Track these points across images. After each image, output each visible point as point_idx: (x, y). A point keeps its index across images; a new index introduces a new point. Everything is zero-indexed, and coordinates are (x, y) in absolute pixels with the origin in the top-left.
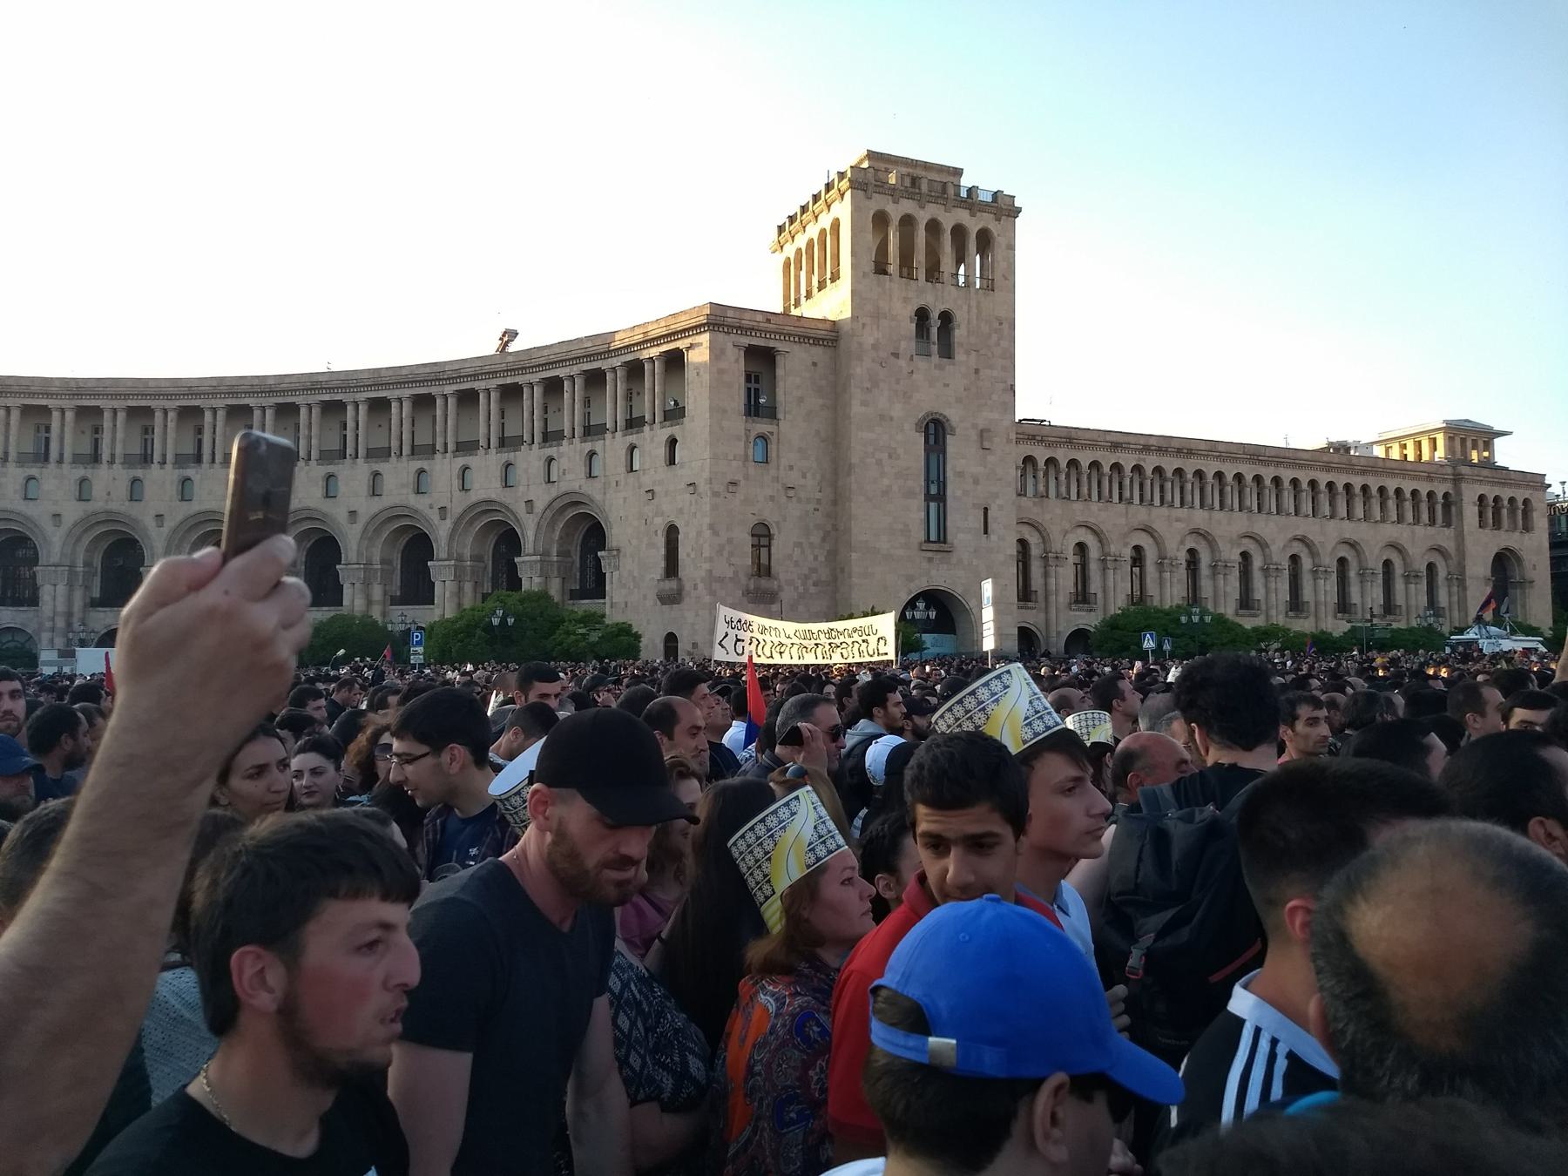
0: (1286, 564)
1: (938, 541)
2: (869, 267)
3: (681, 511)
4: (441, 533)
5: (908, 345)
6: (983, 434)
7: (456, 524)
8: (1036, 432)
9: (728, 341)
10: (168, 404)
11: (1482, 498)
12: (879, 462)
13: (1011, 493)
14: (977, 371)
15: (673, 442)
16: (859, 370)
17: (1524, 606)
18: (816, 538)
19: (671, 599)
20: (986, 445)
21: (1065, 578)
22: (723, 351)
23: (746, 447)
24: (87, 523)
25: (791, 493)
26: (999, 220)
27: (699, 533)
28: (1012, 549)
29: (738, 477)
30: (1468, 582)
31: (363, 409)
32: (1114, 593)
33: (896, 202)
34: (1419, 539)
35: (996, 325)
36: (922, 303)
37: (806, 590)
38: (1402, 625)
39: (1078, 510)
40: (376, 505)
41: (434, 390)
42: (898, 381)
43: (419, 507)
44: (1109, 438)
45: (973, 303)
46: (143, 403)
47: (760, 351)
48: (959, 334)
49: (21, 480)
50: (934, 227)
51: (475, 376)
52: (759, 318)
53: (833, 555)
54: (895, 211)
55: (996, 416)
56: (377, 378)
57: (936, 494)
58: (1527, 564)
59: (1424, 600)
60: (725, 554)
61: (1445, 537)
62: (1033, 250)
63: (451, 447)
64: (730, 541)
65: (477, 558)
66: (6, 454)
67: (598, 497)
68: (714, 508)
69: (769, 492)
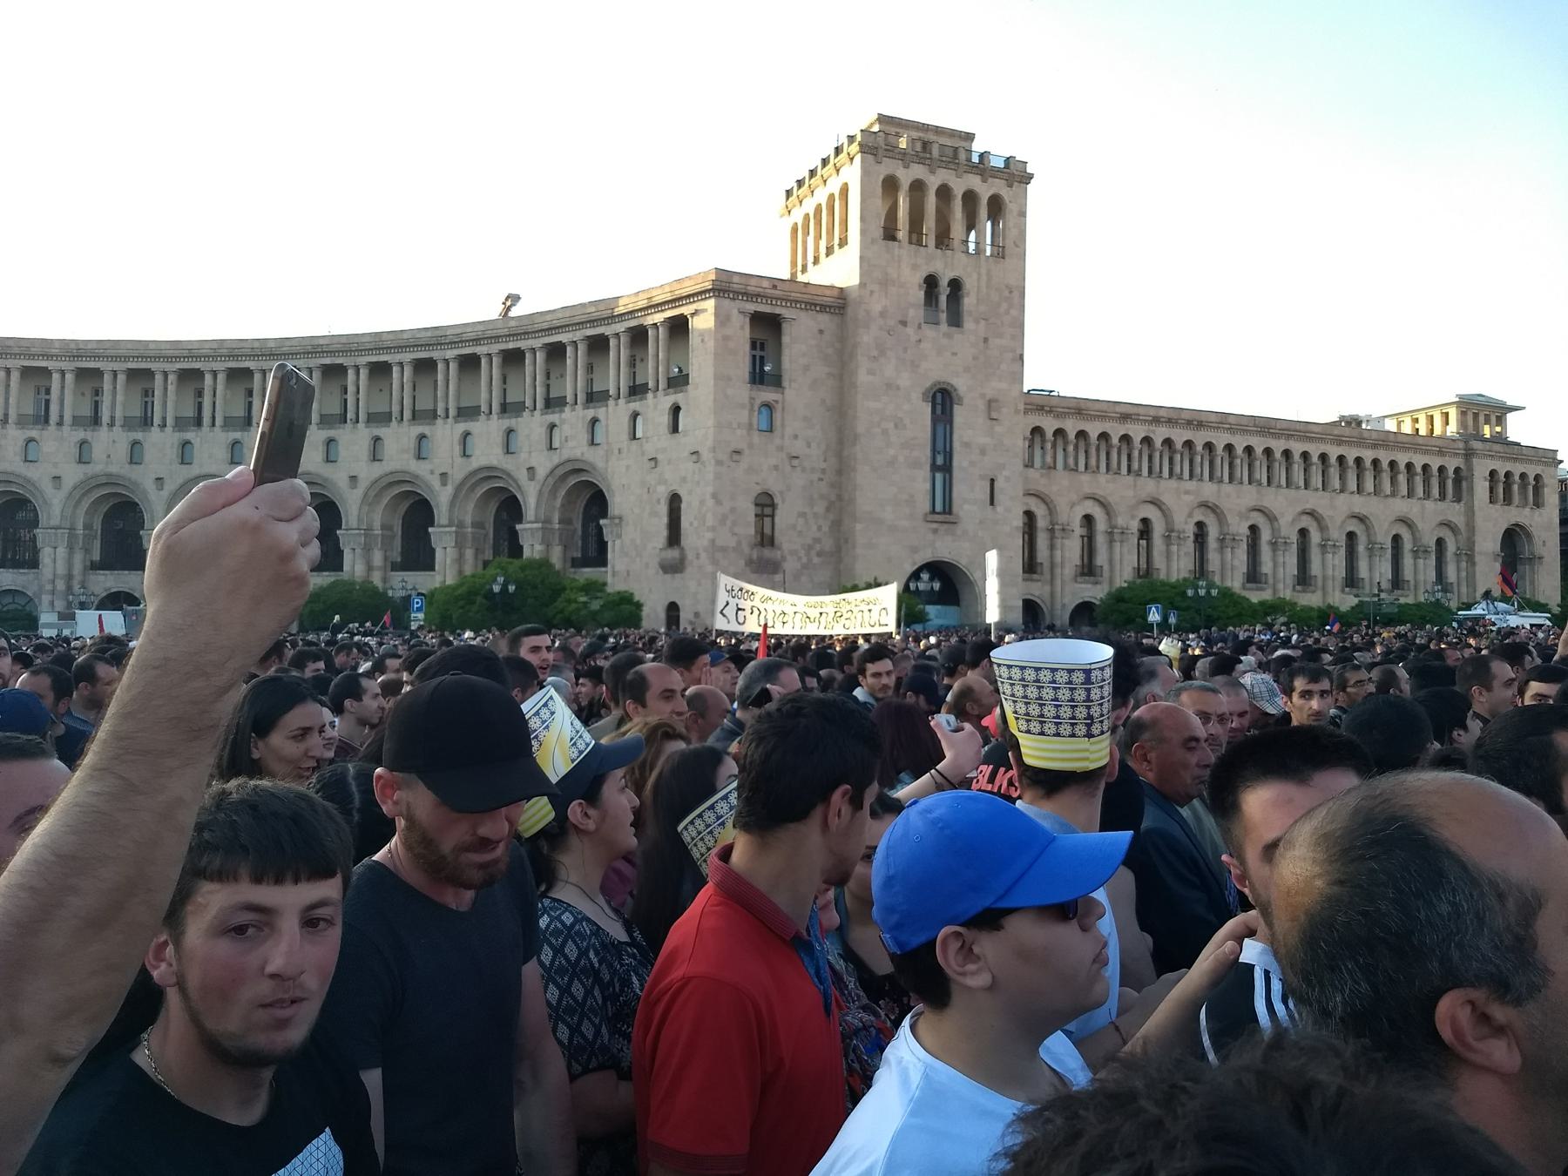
0: (1294, 538)
1: (944, 512)
2: (878, 233)
3: (684, 480)
4: (442, 499)
5: (917, 313)
6: (991, 404)
7: (458, 489)
8: (1043, 403)
9: (733, 307)
10: (168, 367)
11: (1493, 473)
12: (885, 432)
13: (1018, 464)
14: (986, 340)
15: (676, 410)
16: (867, 338)
17: (1532, 583)
18: (820, 508)
19: (673, 568)
20: (994, 415)
21: (1071, 551)
24: (86, 486)
25: (795, 462)
26: (1010, 186)
27: (702, 502)
28: (1018, 521)
29: (742, 445)
30: (1477, 558)
31: (364, 373)
32: (1121, 566)
33: (907, 167)
34: (1428, 514)
35: (1006, 293)
37: (810, 560)
38: (1410, 600)
39: (1087, 483)
40: (377, 470)
41: (435, 355)
42: (905, 350)
43: (420, 472)
44: (1118, 409)
45: (983, 271)
46: (143, 365)
47: (766, 319)
48: (968, 302)
49: (21, 443)
50: (944, 192)
51: (476, 341)
52: (766, 284)
53: (837, 525)
54: (906, 177)
55: (1004, 385)
56: (378, 342)
57: (943, 464)
58: (1537, 541)
59: (1432, 575)
60: (729, 523)
61: (1455, 512)
62: (1045, 216)
63: (452, 412)
64: (733, 510)
65: (478, 525)
66: (6, 415)
67: (600, 464)
68: (718, 476)
69: (773, 461)
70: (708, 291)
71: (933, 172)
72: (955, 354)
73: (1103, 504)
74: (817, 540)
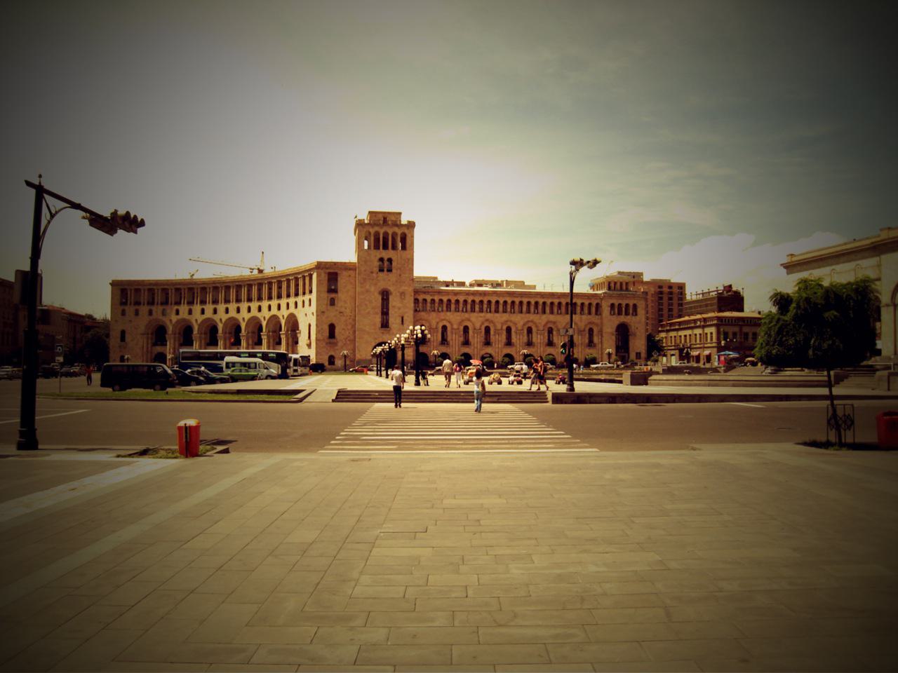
5: (376, 269)
9: (322, 272)
12: (366, 305)
14: (400, 275)
18: (349, 327)
22: (321, 275)
24: (178, 321)
30: (604, 335)
33: (373, 227)
47: (331, 275)
48: (394, 264)
51: (272, 278)
54: (372, 231)
55: (406, 288)
57: (385, 313)
58: (633, 328)
61: (594, 318)
64: (322, 329)
71: (381, 228)
73: (449, 322)
74: (349, 337)
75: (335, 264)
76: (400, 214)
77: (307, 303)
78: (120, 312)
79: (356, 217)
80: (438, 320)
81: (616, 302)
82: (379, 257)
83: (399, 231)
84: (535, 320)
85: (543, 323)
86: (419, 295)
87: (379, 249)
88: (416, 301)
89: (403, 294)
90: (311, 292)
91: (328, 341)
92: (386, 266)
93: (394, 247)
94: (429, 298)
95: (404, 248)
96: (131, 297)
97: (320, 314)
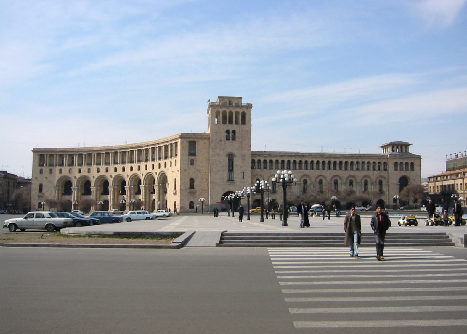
9: (185, 141)
11: (396, 163)
12: (217, 164)
14: (241, 143)
18: (205, 181)
23: (188, 162)
24: (81, 178)
25: (199, 171)
29: (186, 168)
30: (390, 185)
34: (374, 175)
36: (227, 129)
46: (90, 152)
47: (191, 142)
51: (148, 146)
52: (192, 135)
54: (221, 110)
57: (231, 169)
58: (411, 179)
61: (384, 173)
67: (166, 172)
70: (178, 138)
71: (228, 108)
72: (234, 146)
74: (204, 188)
75: (194, 134)
76: (241, 98)
77: (173, 163)
78: (39, 171)
79: (209, 101)
80: (269, 175)
81: (399, 161)
82: (226, 129)
83: (241, 111)
84: (340, 175)
85: (346, 177)
86: (255, 157)
87: (226, 123)
88: (253, 161)
89: (244, 156)
90: (176, 155)
91: (188, 190)
92: (231, 136)
93: (237, 123)
94: (262, 160)
95: (244, 122)
96: (47, 160)
97: (183, 171)
